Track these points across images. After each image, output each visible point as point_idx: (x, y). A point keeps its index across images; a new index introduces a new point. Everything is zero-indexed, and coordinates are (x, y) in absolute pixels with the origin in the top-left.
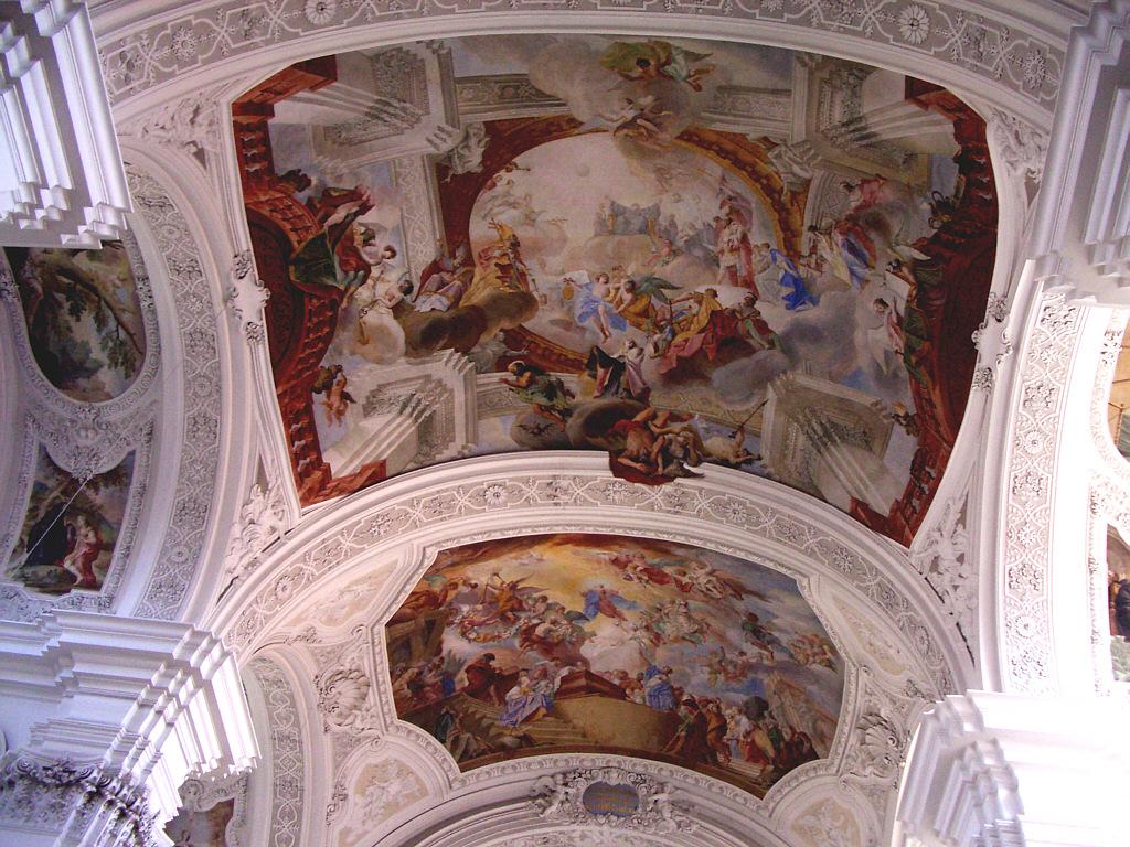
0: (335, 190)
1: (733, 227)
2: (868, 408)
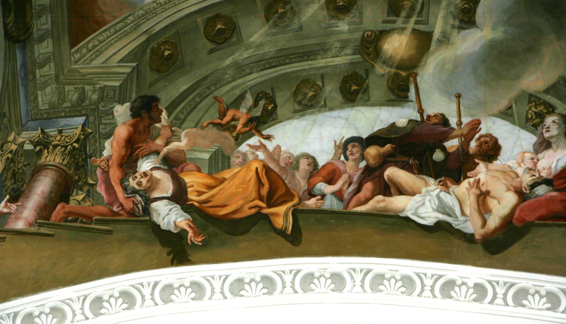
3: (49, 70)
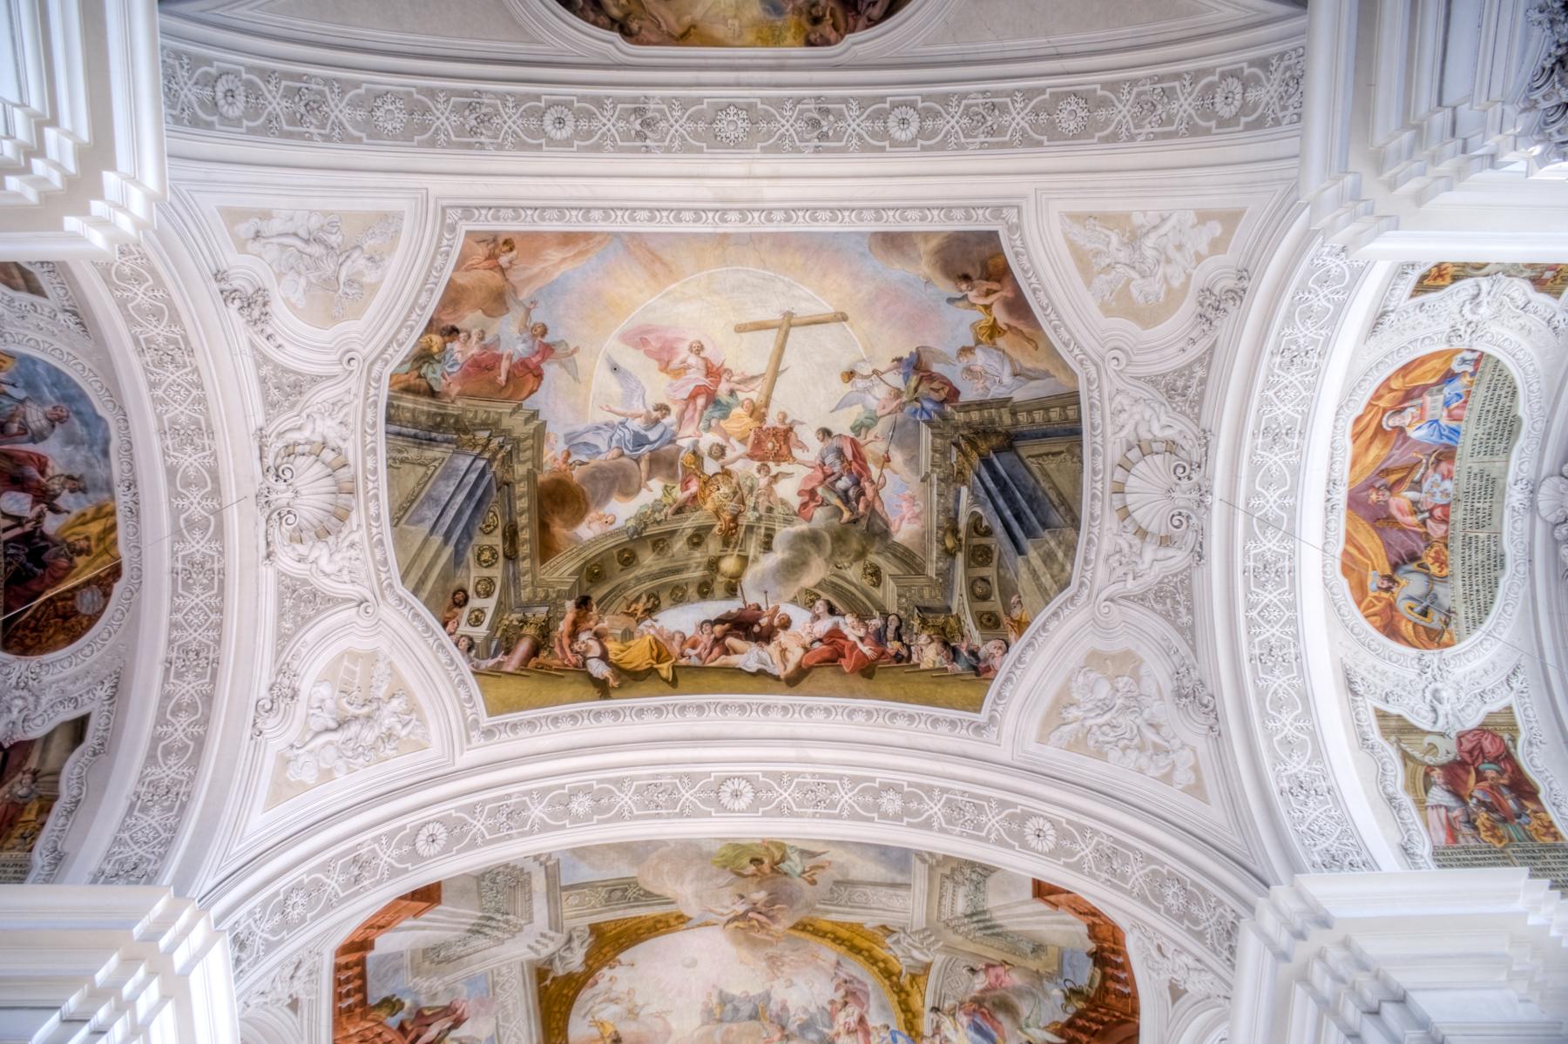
0: (429, 1008)
1: (850, 1009)
3: (528, 578)
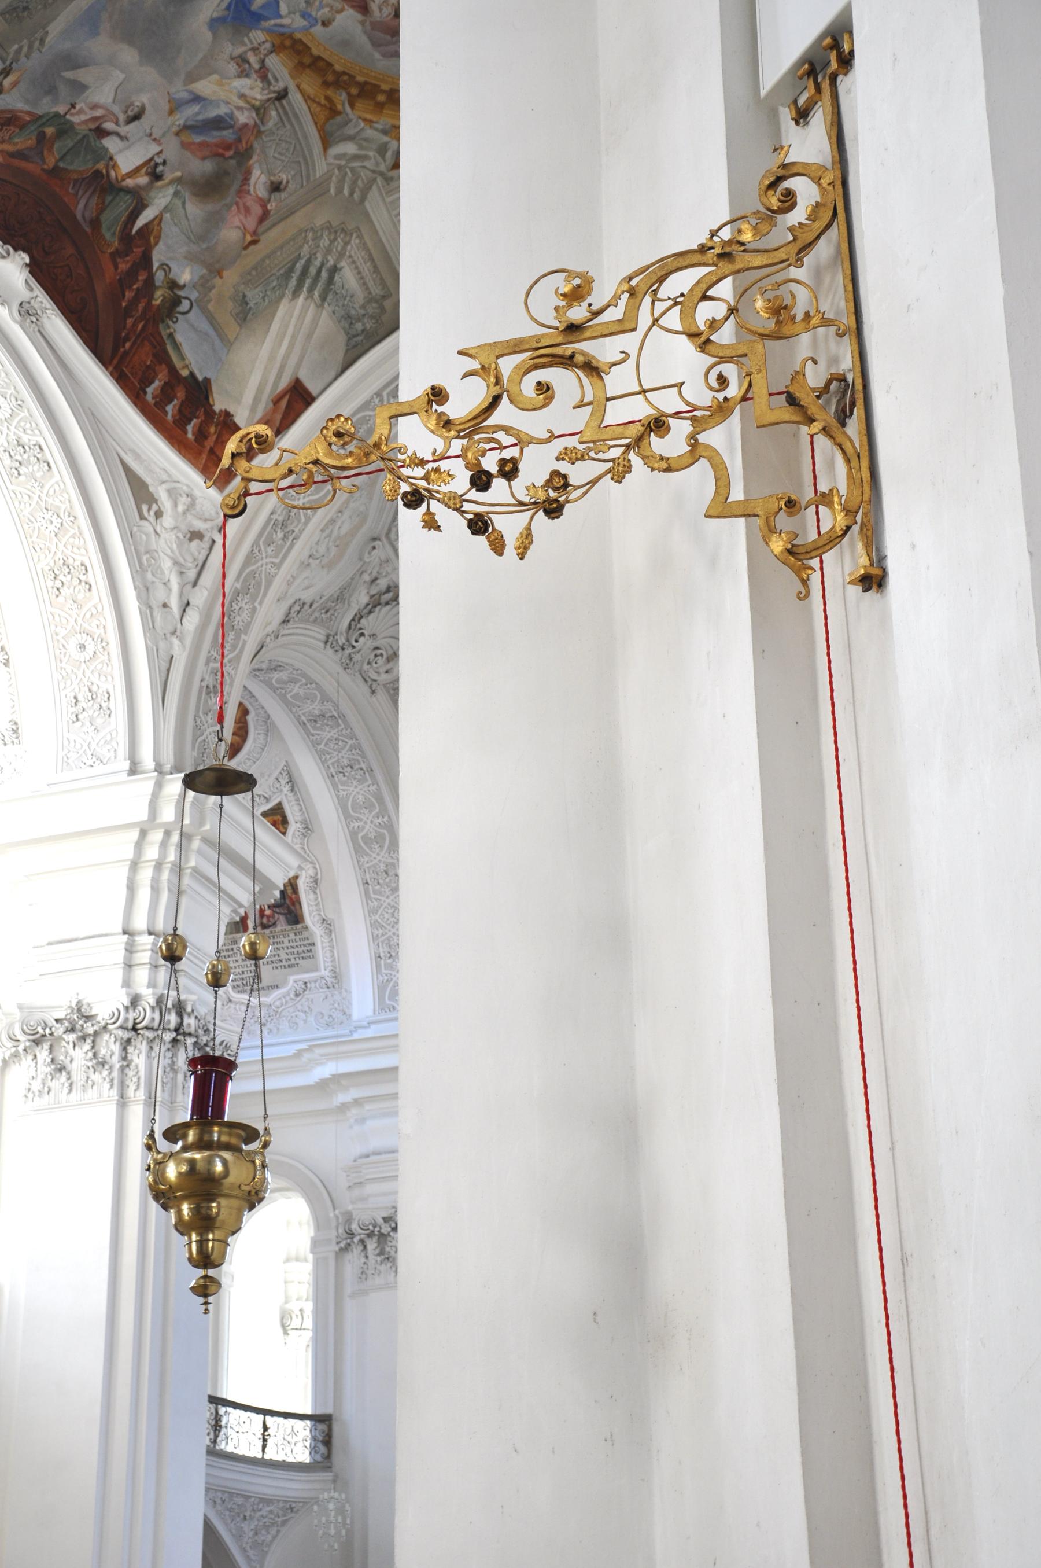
2: (44, 27)
